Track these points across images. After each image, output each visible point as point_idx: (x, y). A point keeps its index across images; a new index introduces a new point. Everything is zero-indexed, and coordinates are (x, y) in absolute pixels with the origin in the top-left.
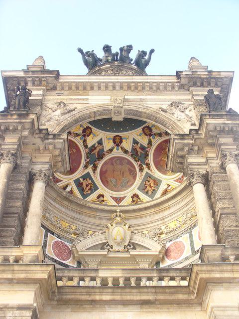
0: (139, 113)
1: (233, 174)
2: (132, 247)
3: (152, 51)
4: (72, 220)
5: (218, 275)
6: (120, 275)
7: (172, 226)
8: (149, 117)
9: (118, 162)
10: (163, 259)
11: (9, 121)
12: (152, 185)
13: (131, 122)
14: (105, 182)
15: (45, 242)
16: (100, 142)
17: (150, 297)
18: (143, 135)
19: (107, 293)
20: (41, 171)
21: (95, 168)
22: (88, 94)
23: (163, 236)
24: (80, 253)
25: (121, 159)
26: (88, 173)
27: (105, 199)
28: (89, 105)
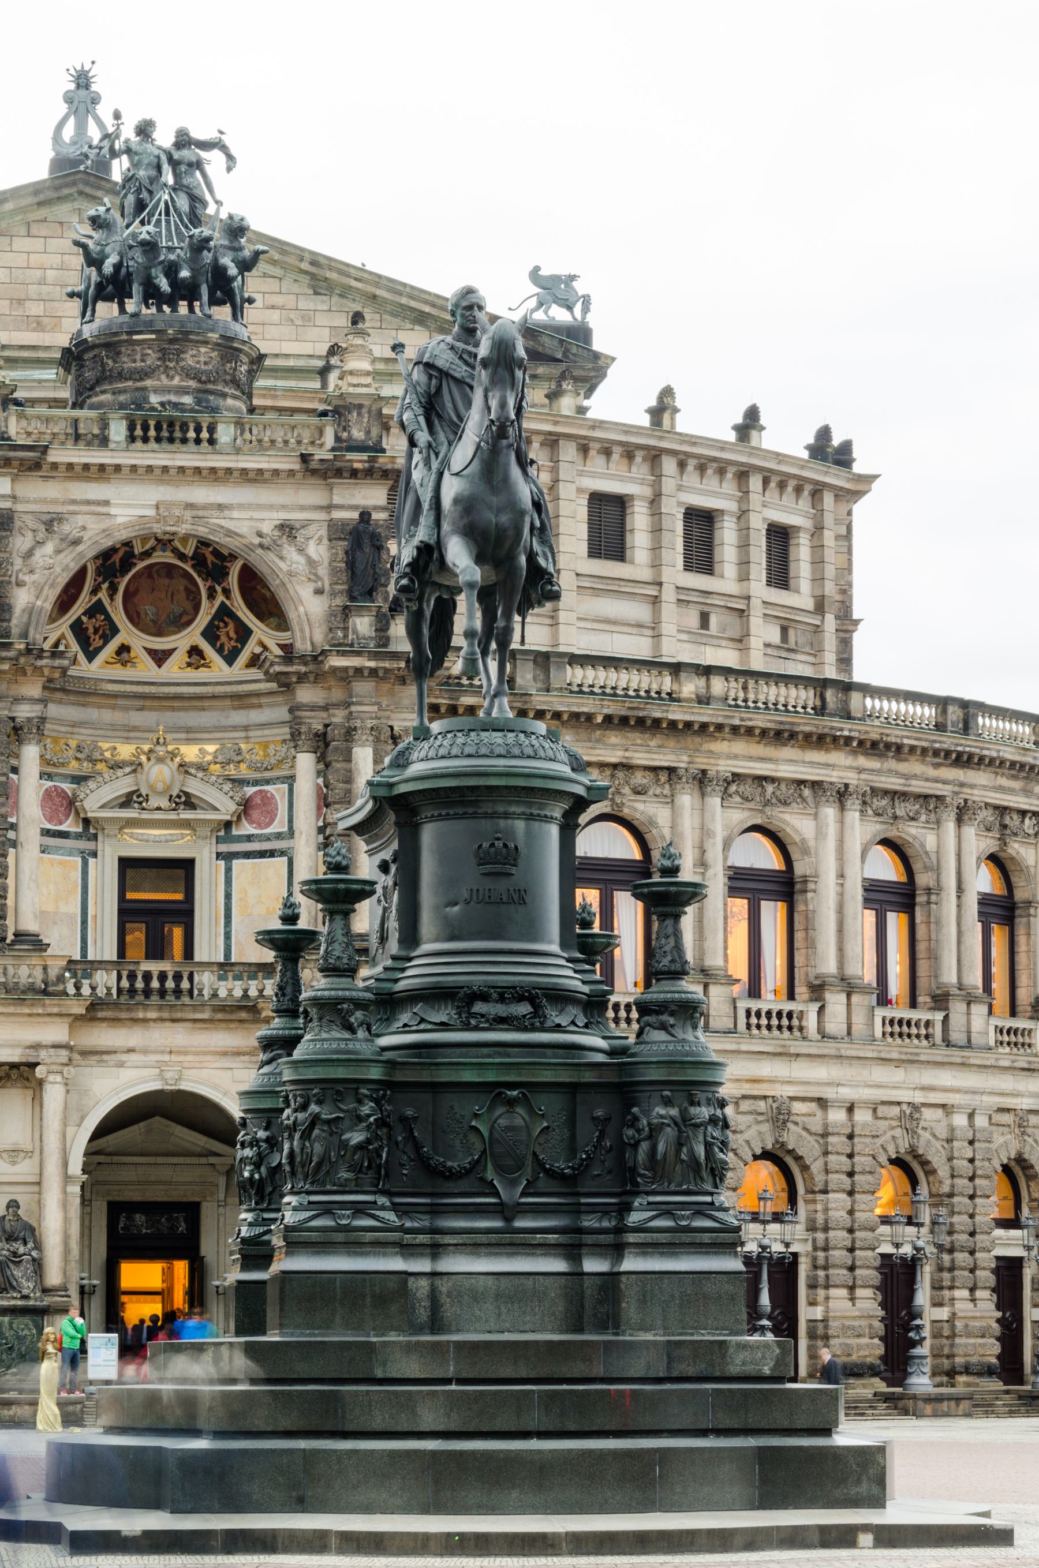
2: (183, 799)
10: (239, 818)
14: (134, 618)
20: (29, 720)
21: (113, 590)
22: (108, 480)
23: (243, 766)
24: (90, 815)
26: (100, 600)
27: (132, 654)
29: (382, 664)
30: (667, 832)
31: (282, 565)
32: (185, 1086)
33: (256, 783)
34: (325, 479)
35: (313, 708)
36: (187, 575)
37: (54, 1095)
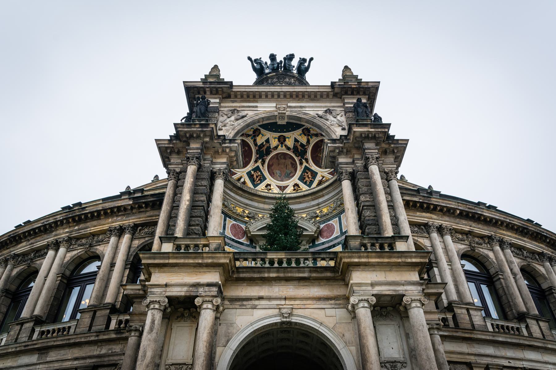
0: (300, 119)
1: (373, 174)
3: (311, 59)
4: (245, 206)
5: (356, 260)
6: (284, 257)
7: (325, 210)
8: (308, 121)
9: (282, 157)
10: (318, 237)
11: (193, 129)
12: (310, 176)
13: (293, 125)
14: (272, 174)
15: (225, 225)
16: (268, 141)
17: (306, 275)
18: (303, 135)
19: (273, 272)
20: (220, 170)
21: (263, 163)
22: (257, 102)
23: (318, 219)
24: (252, 233)
25: (285, 155)
26: (258, 166)
28: (259, 112)
29: (377, 130)
30: (495, 260)
31: (328, 123)
32: (294, 319)
33: (324, 222)
34: (341, 98)
35: (347, 164)
36: (292, 158)
37: (207, 317)
